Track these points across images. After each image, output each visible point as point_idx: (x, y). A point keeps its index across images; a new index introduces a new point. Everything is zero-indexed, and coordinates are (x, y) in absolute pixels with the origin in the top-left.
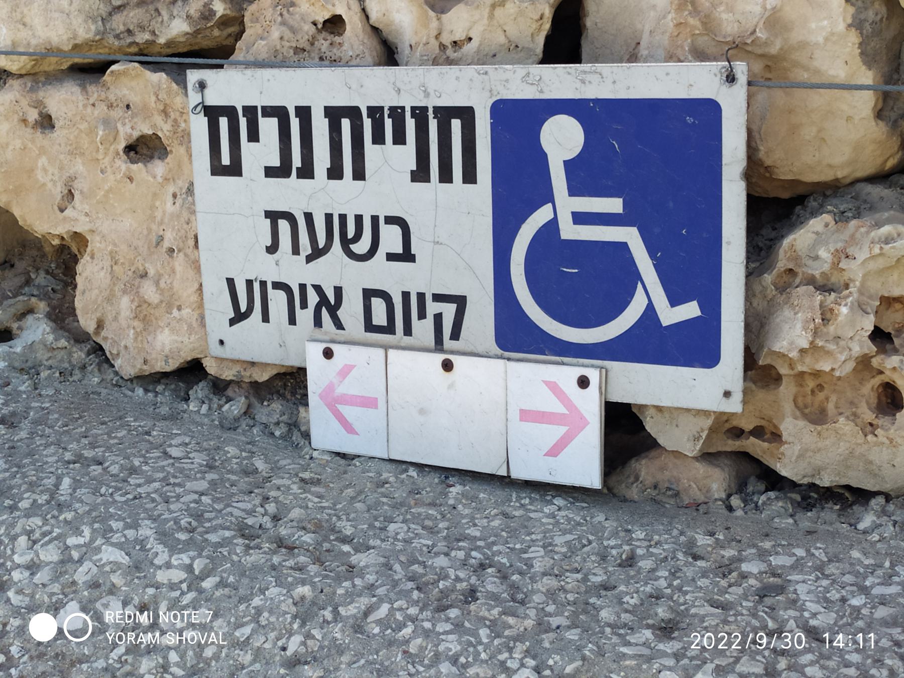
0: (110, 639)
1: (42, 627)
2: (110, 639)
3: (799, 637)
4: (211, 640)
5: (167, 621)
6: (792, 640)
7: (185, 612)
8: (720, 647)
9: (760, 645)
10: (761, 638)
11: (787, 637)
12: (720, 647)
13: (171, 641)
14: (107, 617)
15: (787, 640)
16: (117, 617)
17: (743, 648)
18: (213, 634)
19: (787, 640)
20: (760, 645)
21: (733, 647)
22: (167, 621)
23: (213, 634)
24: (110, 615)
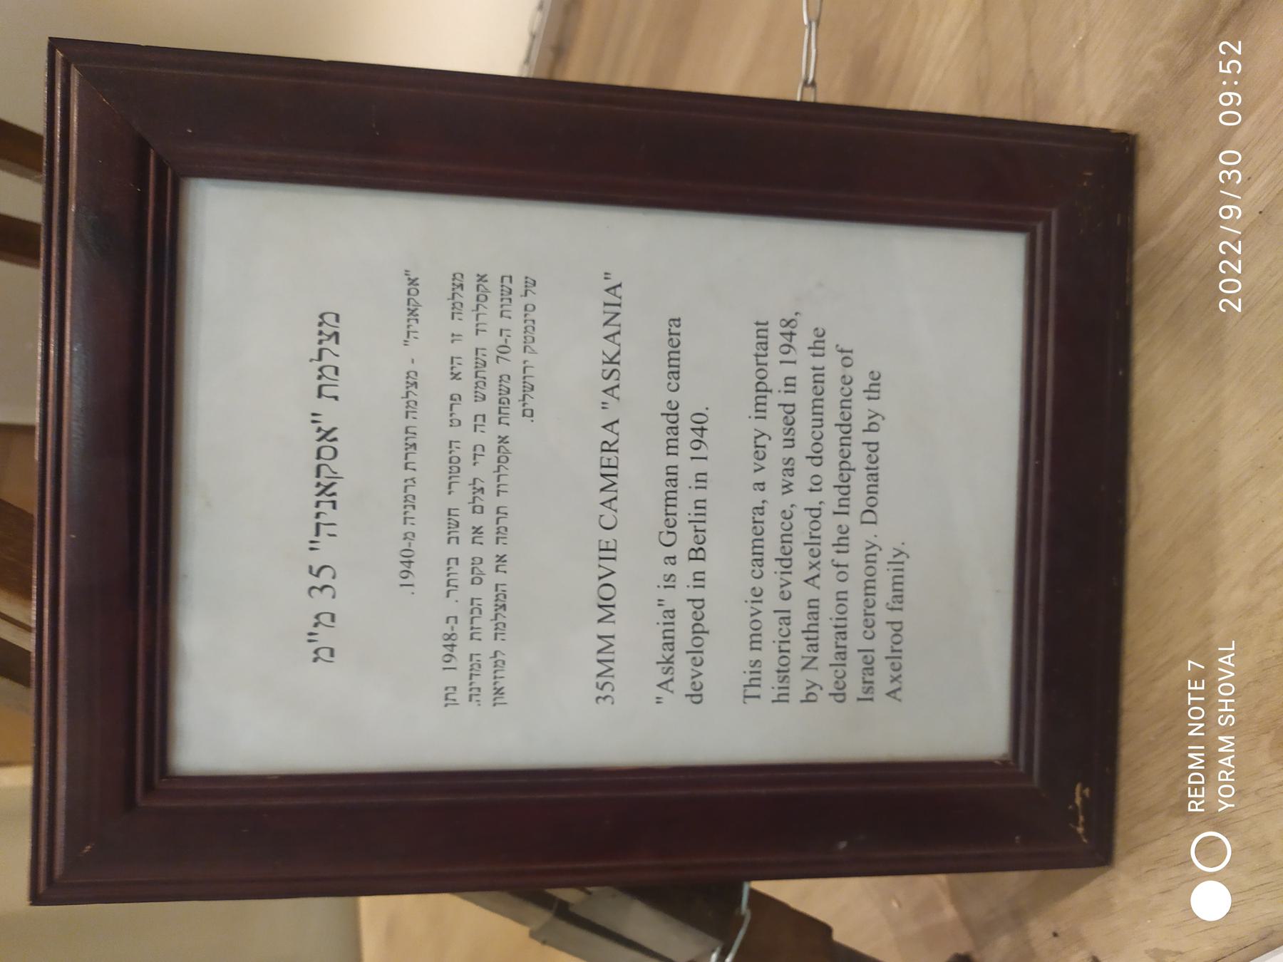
0: (1227, 805)
1: (1211, 901)
2: (1227, 805)
3: (1226, 158)
4: (1229, 663)
5: (1202, 725)
6: (1229, 168)
7: (1190, 699)
8: (1239, 271)
9: (1236, 212)
10: (1226, 212)
11: (1225, 176)
12: (1239, 271)
13: (1230, 720)
14: (1197, 810)
15: (1229, 175)
16: (1196, 796)
17: (1240, 237)
18: (1221, 660)
19: (1229, 175)
20: (1236, 212)
21: (1239, 252)
22: (1202, 725)
23: (1221, 660)
24: (1193, 806)
